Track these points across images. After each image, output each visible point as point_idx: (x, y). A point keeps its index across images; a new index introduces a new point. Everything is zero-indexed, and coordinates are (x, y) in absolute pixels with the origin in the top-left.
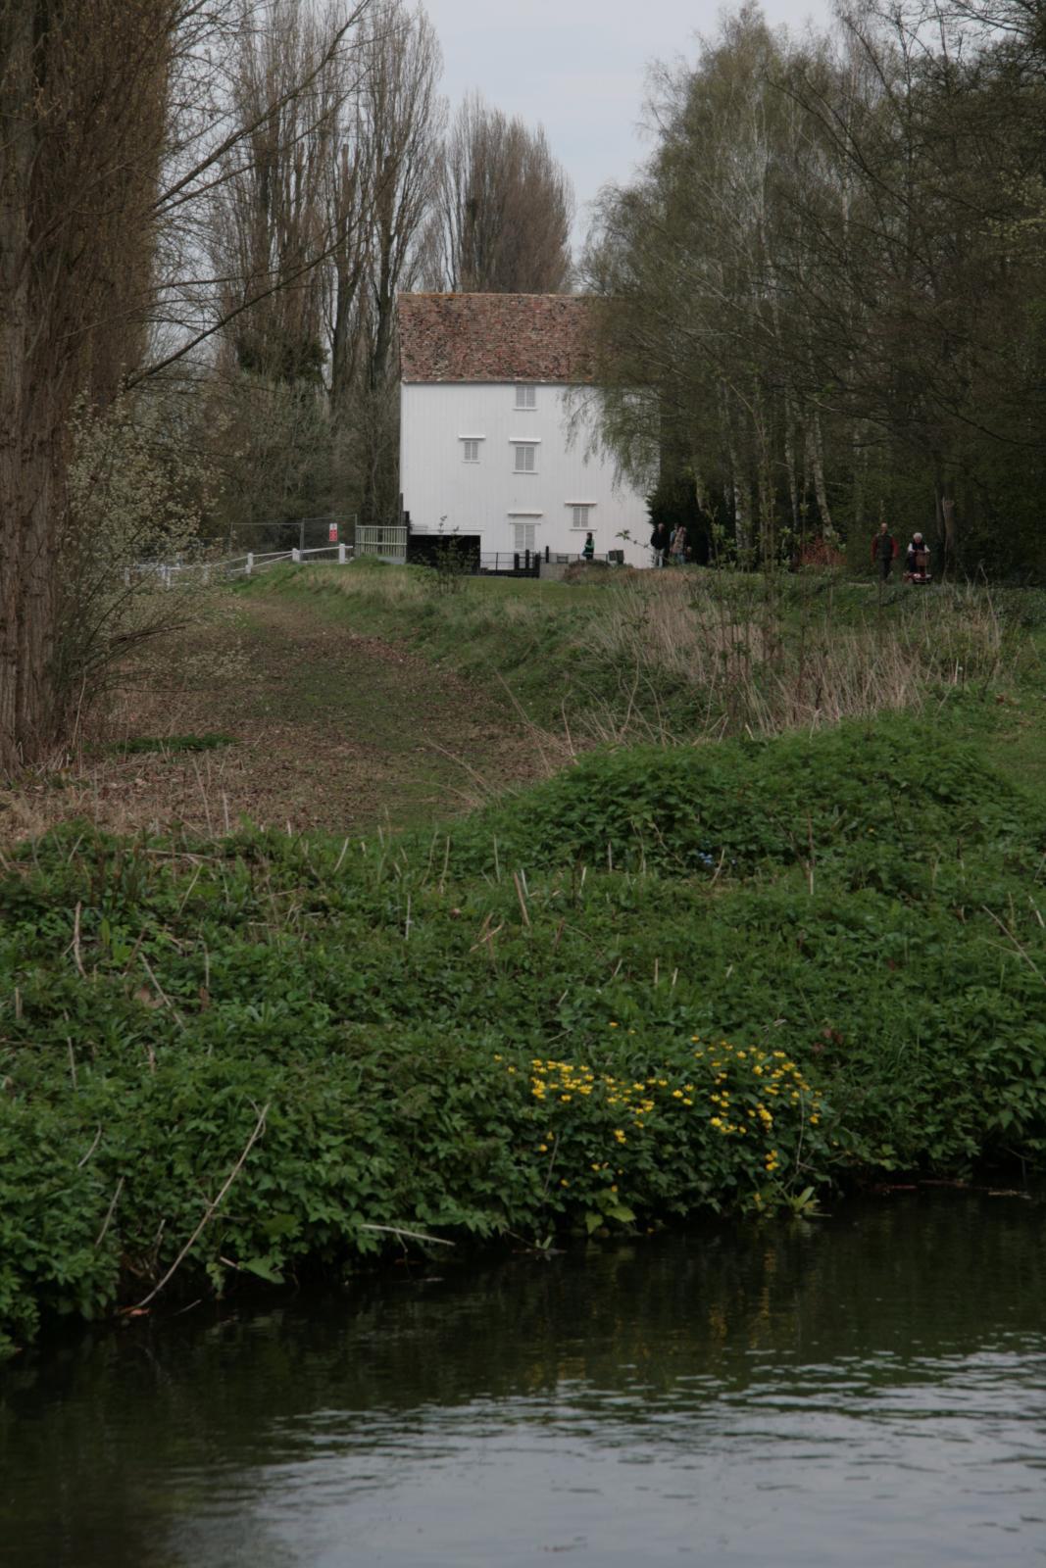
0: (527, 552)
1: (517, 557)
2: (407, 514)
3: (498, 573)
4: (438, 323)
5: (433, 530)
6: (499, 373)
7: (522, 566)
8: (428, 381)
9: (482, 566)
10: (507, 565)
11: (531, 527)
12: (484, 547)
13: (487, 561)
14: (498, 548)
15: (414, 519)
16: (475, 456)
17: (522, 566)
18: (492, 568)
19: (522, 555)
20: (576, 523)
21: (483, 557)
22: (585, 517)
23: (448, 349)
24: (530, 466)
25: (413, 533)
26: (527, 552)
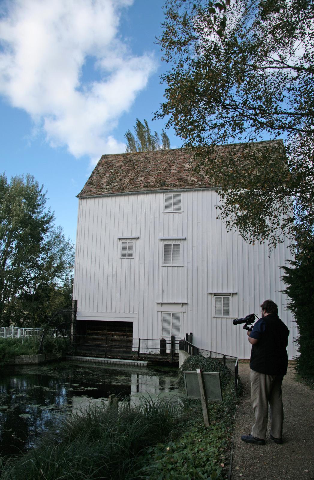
0: (173, 338)
1: (163, 343)
3: (140, 356)
6: (152, 186)
7: (168, 351)
9: (133, 349)
11: (176, 315)
14: (147, 337)
16: (130, 253)
17: (168, 351)
19: (168, 340)
22: (227, 305)
23: (121, 177)
24: (176, 261)
25: (78, 318)
26: (173, 338)
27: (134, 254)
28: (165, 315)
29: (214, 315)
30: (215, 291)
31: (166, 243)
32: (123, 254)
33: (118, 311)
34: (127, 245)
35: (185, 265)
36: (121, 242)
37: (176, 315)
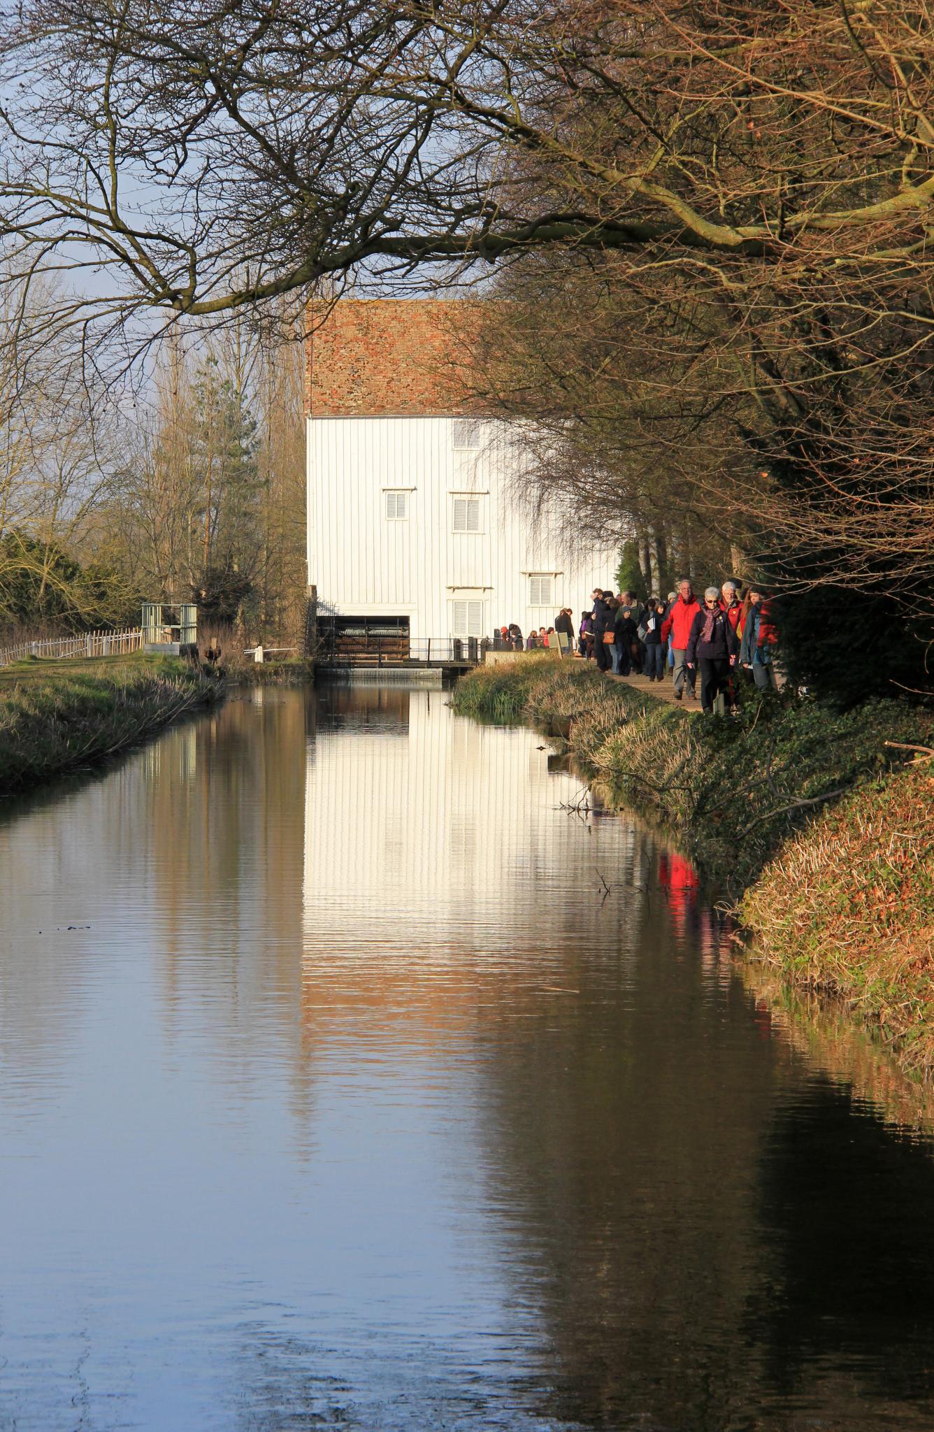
1: (458, 645)
2: (314, 588)
3: (430, 664)
4: (357, 340)
5: (345, 610)
7: (465, 655)
8: (339, 412)
10: (443, 654)
12: (415, 631)
13: (417, 650)
15: (322, 596)
16: (401, 511)
17: (465, 655)
18: (423, 657)
20: (534, 599)
21: (413, 644)
23: (367, 372)
24: (472, 525)
27: (407, 513)
28: (458, 605)
29: (529, 603)
30: (530, 571)
31: (457, 497)
32: (390, 513)
33: (385, 600)
34: (395, 501)
35: (487, 532)
36: (384, 495)
37: (474, 605)
